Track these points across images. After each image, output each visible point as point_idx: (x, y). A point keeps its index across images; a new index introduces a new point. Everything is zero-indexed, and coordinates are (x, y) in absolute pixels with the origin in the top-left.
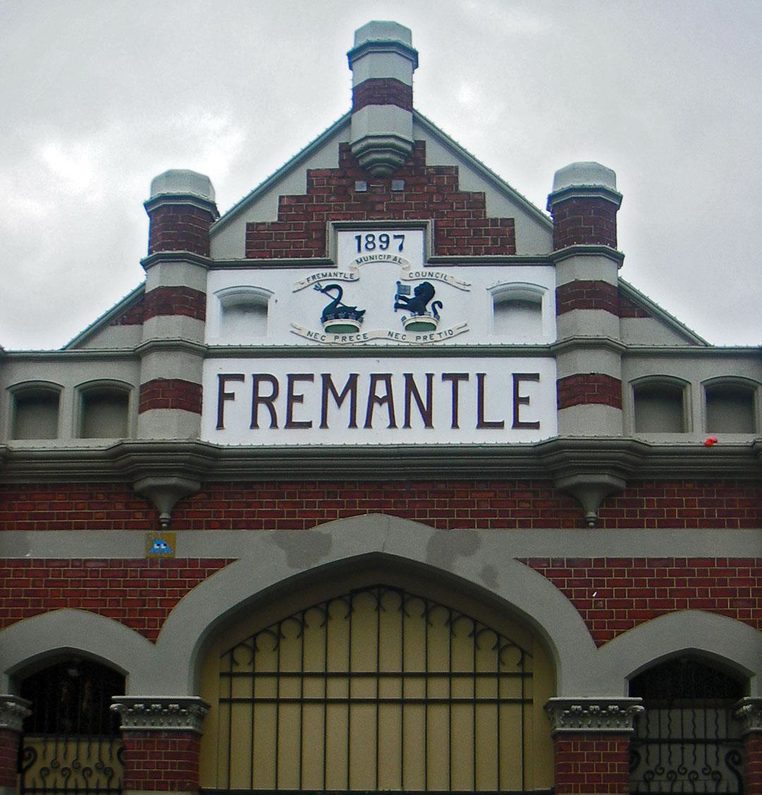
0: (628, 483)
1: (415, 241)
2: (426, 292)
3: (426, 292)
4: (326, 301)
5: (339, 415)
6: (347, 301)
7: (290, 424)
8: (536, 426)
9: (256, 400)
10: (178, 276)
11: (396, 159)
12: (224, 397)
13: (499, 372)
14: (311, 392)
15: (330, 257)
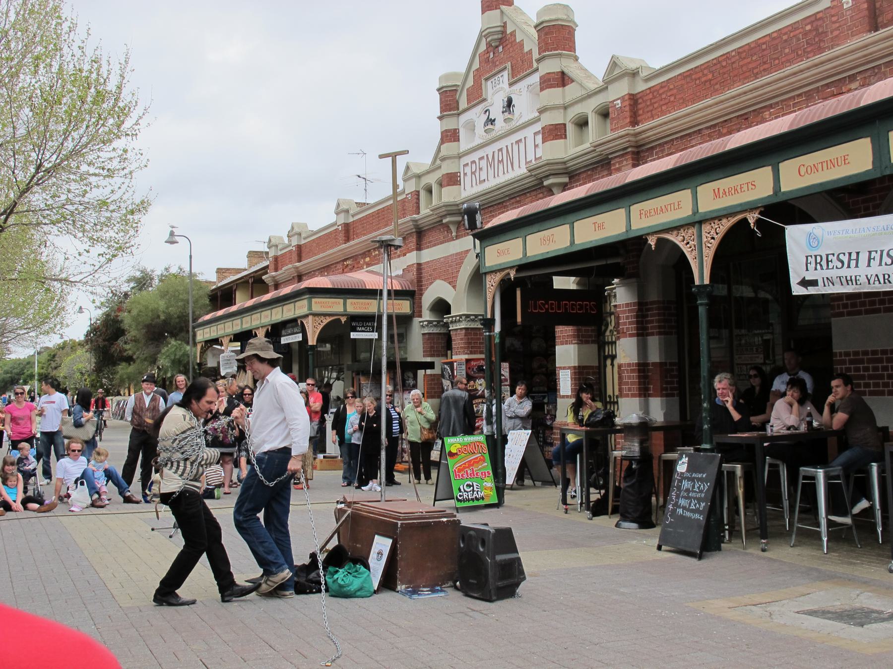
0: (570, 178)
1: (505, 77)
2: (510, 102)
3: (510, 102)
4: (484, 118)
5: (491, 172)
6: (492, 117)
7: (481, 182)
8: (540, 158)
9: (472, 173)
10: (450, 124)
11: (496, 37)
12: (465, 174)
13: (529, 132)
14: (483, 163)
15: (484, 96)
